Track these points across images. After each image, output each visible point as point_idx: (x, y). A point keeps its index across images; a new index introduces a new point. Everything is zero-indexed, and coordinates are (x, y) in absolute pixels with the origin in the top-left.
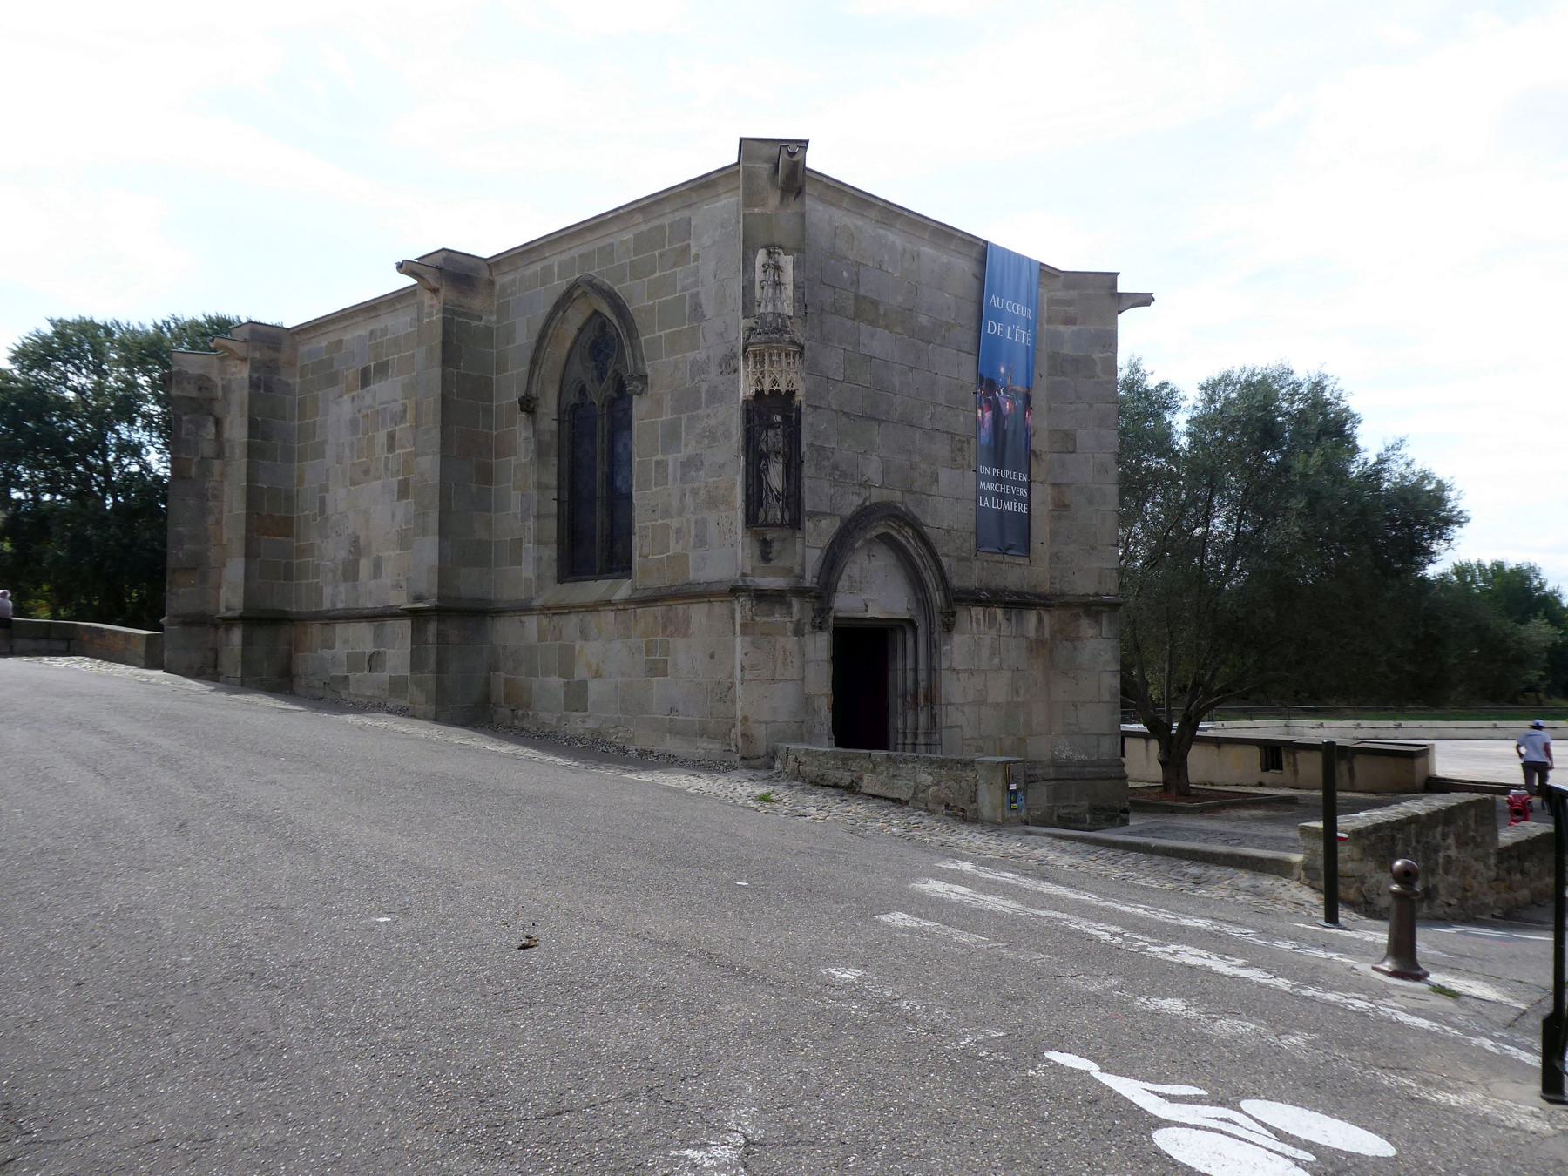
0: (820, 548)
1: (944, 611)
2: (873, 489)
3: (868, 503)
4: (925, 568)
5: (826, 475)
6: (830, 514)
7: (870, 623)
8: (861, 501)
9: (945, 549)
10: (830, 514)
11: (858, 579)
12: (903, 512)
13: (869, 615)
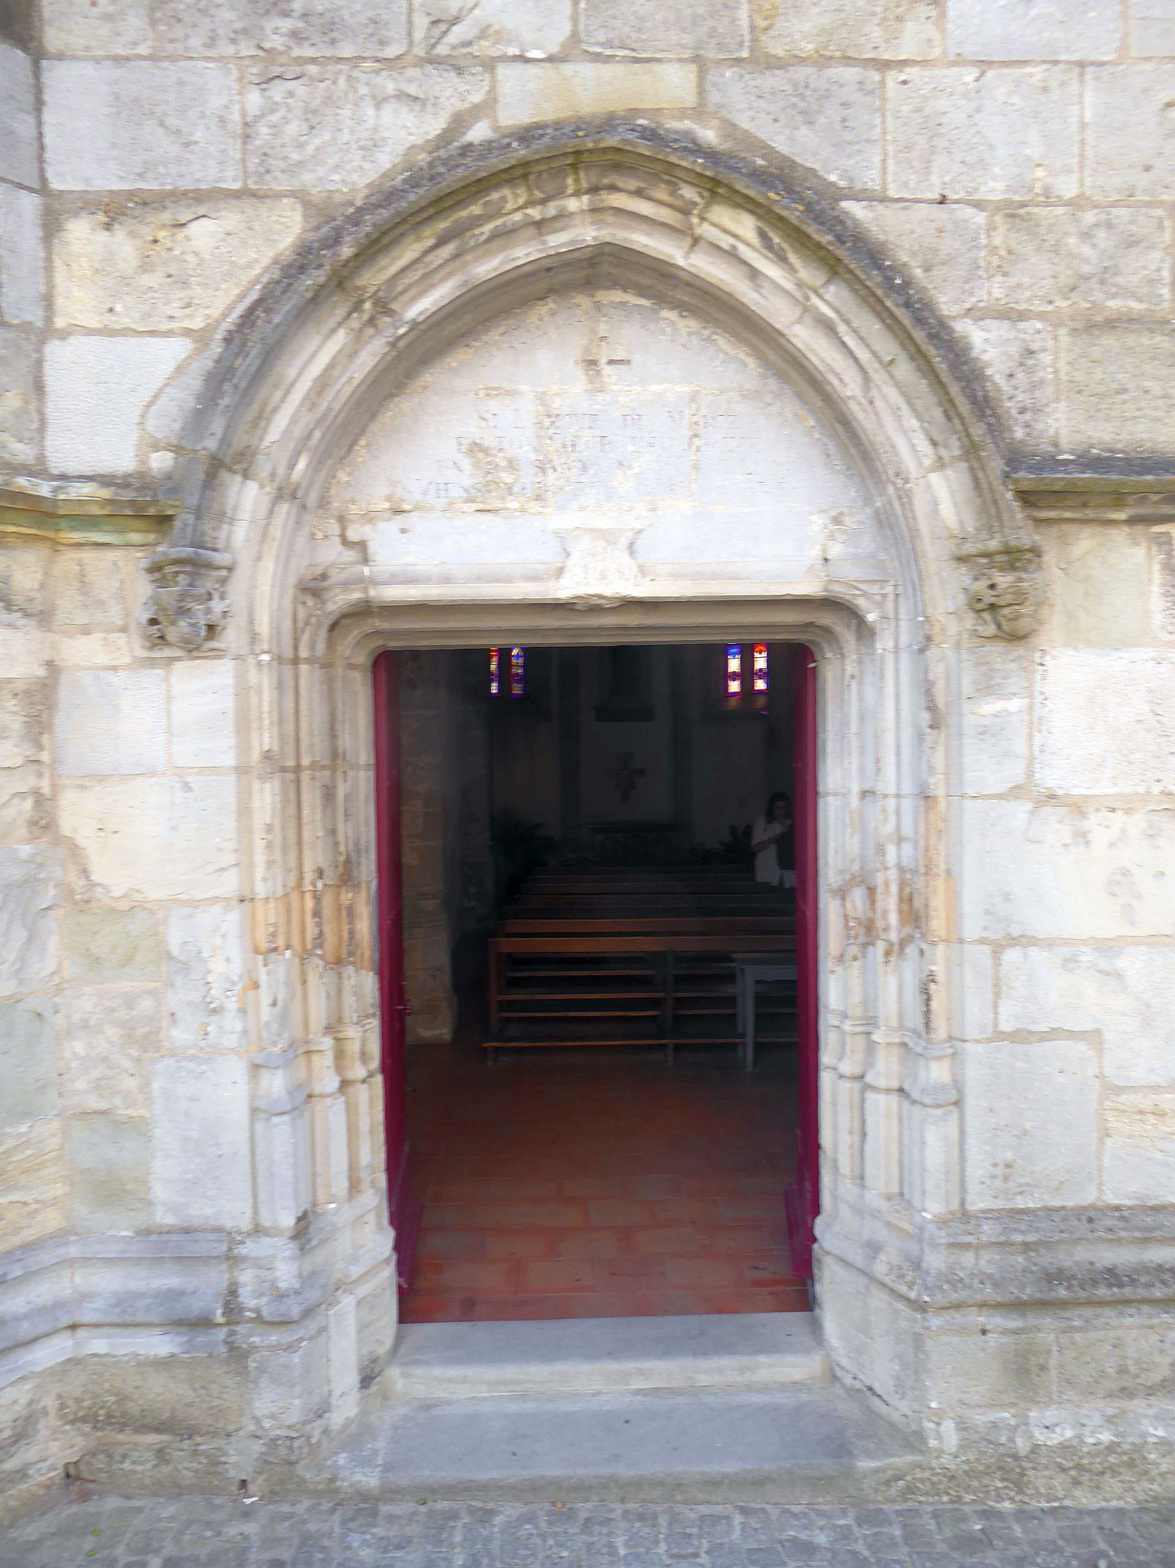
0: (187, 332)
1: (968, 548)
2: (502, 71)
3: (479, 132)
5: (212, 41)
6: (237, 195)
7: (633, 619)
8: (434, 126)
9: (995, 290)
10: (237, 195)
11: (526, 454)
12: (711, 155)
13: (564, 590)
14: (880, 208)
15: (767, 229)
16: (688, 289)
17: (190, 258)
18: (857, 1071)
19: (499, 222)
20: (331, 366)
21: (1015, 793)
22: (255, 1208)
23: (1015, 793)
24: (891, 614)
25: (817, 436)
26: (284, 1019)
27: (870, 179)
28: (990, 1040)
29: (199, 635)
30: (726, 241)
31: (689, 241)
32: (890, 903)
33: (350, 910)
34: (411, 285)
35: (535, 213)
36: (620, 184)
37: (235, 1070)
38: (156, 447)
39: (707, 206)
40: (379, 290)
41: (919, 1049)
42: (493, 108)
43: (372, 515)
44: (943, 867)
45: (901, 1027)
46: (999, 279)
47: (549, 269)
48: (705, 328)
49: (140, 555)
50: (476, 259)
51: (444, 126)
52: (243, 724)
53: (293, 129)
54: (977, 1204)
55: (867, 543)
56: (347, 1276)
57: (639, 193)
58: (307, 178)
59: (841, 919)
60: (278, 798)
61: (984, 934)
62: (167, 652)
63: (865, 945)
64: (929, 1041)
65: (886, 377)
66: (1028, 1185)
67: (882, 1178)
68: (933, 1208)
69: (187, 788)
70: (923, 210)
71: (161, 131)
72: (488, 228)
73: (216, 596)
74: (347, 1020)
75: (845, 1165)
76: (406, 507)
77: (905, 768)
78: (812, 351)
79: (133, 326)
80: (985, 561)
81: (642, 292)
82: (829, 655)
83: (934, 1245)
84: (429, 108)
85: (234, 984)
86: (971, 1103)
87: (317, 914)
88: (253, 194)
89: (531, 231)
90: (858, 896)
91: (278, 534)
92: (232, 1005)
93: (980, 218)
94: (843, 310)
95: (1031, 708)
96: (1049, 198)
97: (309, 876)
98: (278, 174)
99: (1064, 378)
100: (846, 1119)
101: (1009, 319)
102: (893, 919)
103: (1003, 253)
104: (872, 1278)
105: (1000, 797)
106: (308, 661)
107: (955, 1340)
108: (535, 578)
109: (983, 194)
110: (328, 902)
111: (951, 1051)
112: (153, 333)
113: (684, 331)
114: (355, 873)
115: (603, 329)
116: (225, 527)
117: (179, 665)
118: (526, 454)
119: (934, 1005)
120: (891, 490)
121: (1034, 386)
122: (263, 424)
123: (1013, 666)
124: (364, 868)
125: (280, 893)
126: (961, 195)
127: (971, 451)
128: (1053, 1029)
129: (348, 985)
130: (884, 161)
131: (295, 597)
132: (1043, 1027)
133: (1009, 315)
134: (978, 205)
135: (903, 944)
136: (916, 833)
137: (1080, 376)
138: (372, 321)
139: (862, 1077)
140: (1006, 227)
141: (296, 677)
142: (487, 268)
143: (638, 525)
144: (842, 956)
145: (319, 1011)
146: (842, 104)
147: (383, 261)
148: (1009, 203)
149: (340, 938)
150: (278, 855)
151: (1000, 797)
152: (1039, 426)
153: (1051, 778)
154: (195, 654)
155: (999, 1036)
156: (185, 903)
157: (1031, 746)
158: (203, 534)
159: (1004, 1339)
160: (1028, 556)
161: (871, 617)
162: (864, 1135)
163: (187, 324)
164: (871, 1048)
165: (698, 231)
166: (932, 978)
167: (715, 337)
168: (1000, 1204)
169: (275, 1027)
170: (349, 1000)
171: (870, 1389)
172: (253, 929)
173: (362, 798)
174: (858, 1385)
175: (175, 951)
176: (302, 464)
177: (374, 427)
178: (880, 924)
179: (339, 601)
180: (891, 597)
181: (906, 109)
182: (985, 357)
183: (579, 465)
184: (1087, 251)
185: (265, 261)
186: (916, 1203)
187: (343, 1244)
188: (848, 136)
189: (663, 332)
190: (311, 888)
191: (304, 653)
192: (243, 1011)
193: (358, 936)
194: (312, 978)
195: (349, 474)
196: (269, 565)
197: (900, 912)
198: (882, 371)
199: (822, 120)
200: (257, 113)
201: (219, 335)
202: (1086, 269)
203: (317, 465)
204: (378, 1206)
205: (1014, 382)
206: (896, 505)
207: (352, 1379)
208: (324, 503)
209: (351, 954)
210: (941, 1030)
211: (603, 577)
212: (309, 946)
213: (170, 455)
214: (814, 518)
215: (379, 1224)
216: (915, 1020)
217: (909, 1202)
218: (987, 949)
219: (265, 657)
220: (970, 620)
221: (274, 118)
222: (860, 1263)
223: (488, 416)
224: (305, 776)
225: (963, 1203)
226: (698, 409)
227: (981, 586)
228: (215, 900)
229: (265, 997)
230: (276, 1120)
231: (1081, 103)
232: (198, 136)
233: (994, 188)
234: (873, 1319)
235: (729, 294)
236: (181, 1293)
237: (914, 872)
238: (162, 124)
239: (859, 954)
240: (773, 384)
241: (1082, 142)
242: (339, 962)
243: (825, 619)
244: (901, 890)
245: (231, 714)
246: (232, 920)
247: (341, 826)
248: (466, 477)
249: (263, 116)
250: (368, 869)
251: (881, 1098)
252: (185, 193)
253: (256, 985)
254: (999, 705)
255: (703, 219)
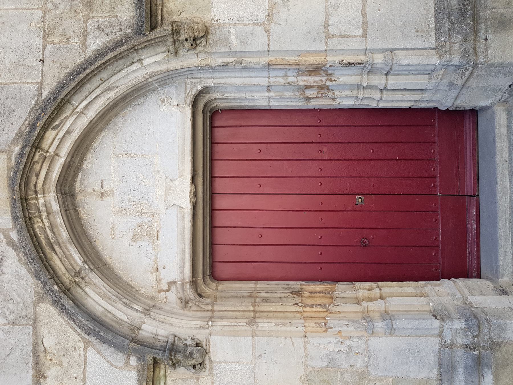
0: (85, 349)
3: (14, 236)
4: (108, 90)
6: (35, 328)
8: (11, 252)
10: (35, 328)
12: (24, 147)
13: (188, 207)
14: (45, 84)
15: (51, 127)
16: (74, 157)
17: (57, 347)
18: (379, 92)
19: (47, 229)
20: (99, 294)
21: (267, 31)
22: (431, 336)
23: (267, 31)
24: (199, 80)
25: (131, 109)
26: (354, 321)
27: (34, 88)
28: (366, 39)
29: (200, 349)
30: (56, 143)
31: (56, 157)
32: (312, 80)
33: (311, 292)
34: (70, 263)
35: (44, 215)
36: (34, 183)
37: (375, 343)
38: (127, 363)
39: (42, 150)
40: (71, 275)
41: (370, 67)
42: (6, 230)
43: (158, 279)
44: (297, 58)
45: (361, 74)
46: (71, 40)
47: (66, 211)
48: (90, 151)
49: (169, 371)
50: (62, 238)
51: (11, 248)
52: (235, 333)
53: (11, 306)
54: (433, 43)
55: (171, 89)
56: (460, 300)
57: (37, 176)
58: (29, 301)
59: (318, 100)
60: (265, 320)
61: (323, 42)
62: (207, 362)
63: (329, 90)
64: (366, 63)
65: (107, 82)
66: (425, 23)
67: (422, 81)
68: (434, 60)
69: (260, 356)
70: (46, 68)
71: (11, 356)
72: (50, 234)
73: (185, 342)
74: (355, 296)
75: (417, 97)
76: (155, 267)
77: (258, 74)
78: (97, 110)
79: (82, 370)
80: (177, 43)
81: (76, 175)
82: (215, 105)
83: (450, 61)
84: (4, 254)
85: (339, 341)
86: (391, 46)
87: (312, 306)
88: (35, 322)
89: (51, 217)
90: (309, 93)
91: (162, 317)
92: (347, 342)
93: (49, 46)
94: (82, 98)
95: (234, 24)
96: (43, 20)
97: (297, 309)
98: (28, 312)
99: (108, 14)
100: (398, 96)
101: (86, 35)
102: (317, 78)
103: (62, 38)
104: (464, 86)
105: (269, 36)
106: (213, 306)
107: (489, 51)
108: (183, 217)
109: (40, 46)
110: (308, 301)
111: (370, 54)
112: (85, 362)
113: (91, 159)
114: (297, 290)
115: (90, 190)
116: (159, 338)
117: (212, 358)
118: (138, 219)
119: (352, 61)
120: (150, 80)
121: (111, 25)
122: (120, 321)
123: (218, 32)
124: (295, 287)
125: (303, 321)
126: (40, 53)
127: (134, 49)
128: (362, 13)
129: (342, 295)
130: (28, 83)
131: (188, 310)
132: (361, 18)
133: (85, 36)
134: (44, 48)
135: (328, 74)
136: (283, 69)
137: (108, 8)
138: (83, 278)
139: (381, 90)
140: (52, 37)
141: (219, 311)
142: (64, 234)
143: (164, 178)
144: (332, 99)
145: (352, 307)
146: (7, 99)
147: (60, 273)
148: (44, 36)
149: (323, 297)
150: (288, 321)
151: (269, 36)
152: (126, 23)
153: (262, 16)
154: (207, 351)
155: (364, 35)
156: (306, 360)
157: (249, 24)
158: (161, 346)
159: (489, 31)
160: (174, 25)
161: (200, 88)
162: (405, 90)
163: (82, 349)
164: (370, 87)
165: (52, 153)
166: (341, 62)
167: (93, 148)
168: (433, 34)
169: (357, 325)
170: (347, 295)
171: (510, 86)
172: (317, 332)
173: (267, 286)
174: (508, 91)
175: (326, 364)
176: (136, 307)
177: (125, 278)
178: (319, 83)
179: (190, 293)
180: (192, 80)
181: (9, 75)
182: (100, 44)
183: (141, 199)
184: (61, 7)
185: (60, 318)
186: (433, 68)
187: (447, 300)
188: (18, 97)
189: (91, 167)
190: (302, 308)
191: (210, 308)
192: (350, 338)
193: (322, 290)
194: (338, 308)
195: (142, 288)
196: (173, 321)
197: (315, 76)
198: (105, 83)
199: (12, 107)
200: (5, 319)
201: (87, 337)
202: (68, 7)
203: (137, 300)
204: (432, 286)
205: (109, 33)
206: (156, 78)
207: (503, 298)
208: (153, 298)
209: (329, 293)
210: (361, 58)
211: (183, 191)
212: (325, 310)
213: (131, 358)
214: (162, 110)
215: (439, 285)
216: (357, 69)
217: (432, 71)
218: (329, 40)
219: (210, 323)
220: (200, 49)
221: (7, 313)
222: (458, 90)
223: (122, 233)
224: (258, 309)
225: (433, 49)
226: (121, 155)
227: (187, 44)
228: (305, 347)
229: (344, 329)
230: (394, 327)
231: (8, 9)
232: (13, 342)
233: (39, 42)
234: (481, 85)
235: (76, 141)
236: (466, 367)
237: (299, 70)
238: (8, 355)
239: (332, 92)
240: (111, 126)
241: (22, 9)
242: (332, 298)
243: (201, 106)
244: (306, 75)
245: (231, 338)
246: (313, 341)
247: (278, 295)
248: (145, 244)
249: (6, 317)
250: (295, 285)
251: (390, 82)
252: (34, 348)
253: (340, 332)
254: (233, 37)
255: (47, 152)
